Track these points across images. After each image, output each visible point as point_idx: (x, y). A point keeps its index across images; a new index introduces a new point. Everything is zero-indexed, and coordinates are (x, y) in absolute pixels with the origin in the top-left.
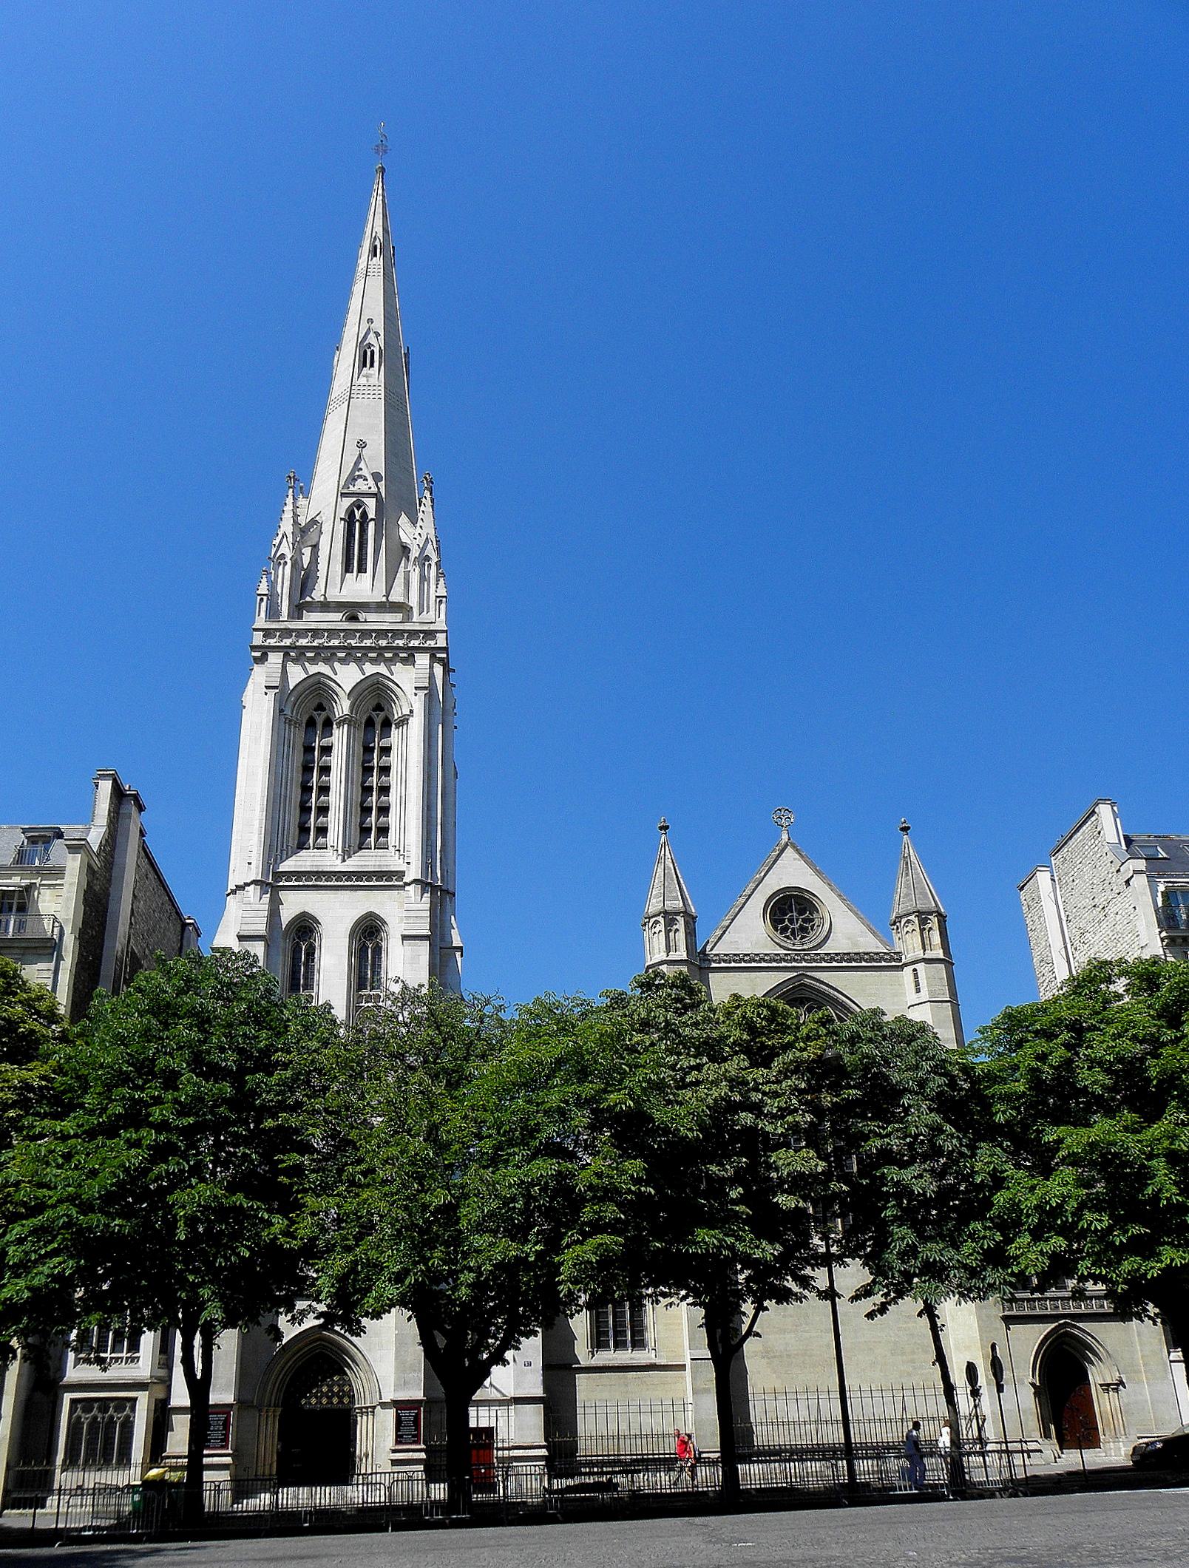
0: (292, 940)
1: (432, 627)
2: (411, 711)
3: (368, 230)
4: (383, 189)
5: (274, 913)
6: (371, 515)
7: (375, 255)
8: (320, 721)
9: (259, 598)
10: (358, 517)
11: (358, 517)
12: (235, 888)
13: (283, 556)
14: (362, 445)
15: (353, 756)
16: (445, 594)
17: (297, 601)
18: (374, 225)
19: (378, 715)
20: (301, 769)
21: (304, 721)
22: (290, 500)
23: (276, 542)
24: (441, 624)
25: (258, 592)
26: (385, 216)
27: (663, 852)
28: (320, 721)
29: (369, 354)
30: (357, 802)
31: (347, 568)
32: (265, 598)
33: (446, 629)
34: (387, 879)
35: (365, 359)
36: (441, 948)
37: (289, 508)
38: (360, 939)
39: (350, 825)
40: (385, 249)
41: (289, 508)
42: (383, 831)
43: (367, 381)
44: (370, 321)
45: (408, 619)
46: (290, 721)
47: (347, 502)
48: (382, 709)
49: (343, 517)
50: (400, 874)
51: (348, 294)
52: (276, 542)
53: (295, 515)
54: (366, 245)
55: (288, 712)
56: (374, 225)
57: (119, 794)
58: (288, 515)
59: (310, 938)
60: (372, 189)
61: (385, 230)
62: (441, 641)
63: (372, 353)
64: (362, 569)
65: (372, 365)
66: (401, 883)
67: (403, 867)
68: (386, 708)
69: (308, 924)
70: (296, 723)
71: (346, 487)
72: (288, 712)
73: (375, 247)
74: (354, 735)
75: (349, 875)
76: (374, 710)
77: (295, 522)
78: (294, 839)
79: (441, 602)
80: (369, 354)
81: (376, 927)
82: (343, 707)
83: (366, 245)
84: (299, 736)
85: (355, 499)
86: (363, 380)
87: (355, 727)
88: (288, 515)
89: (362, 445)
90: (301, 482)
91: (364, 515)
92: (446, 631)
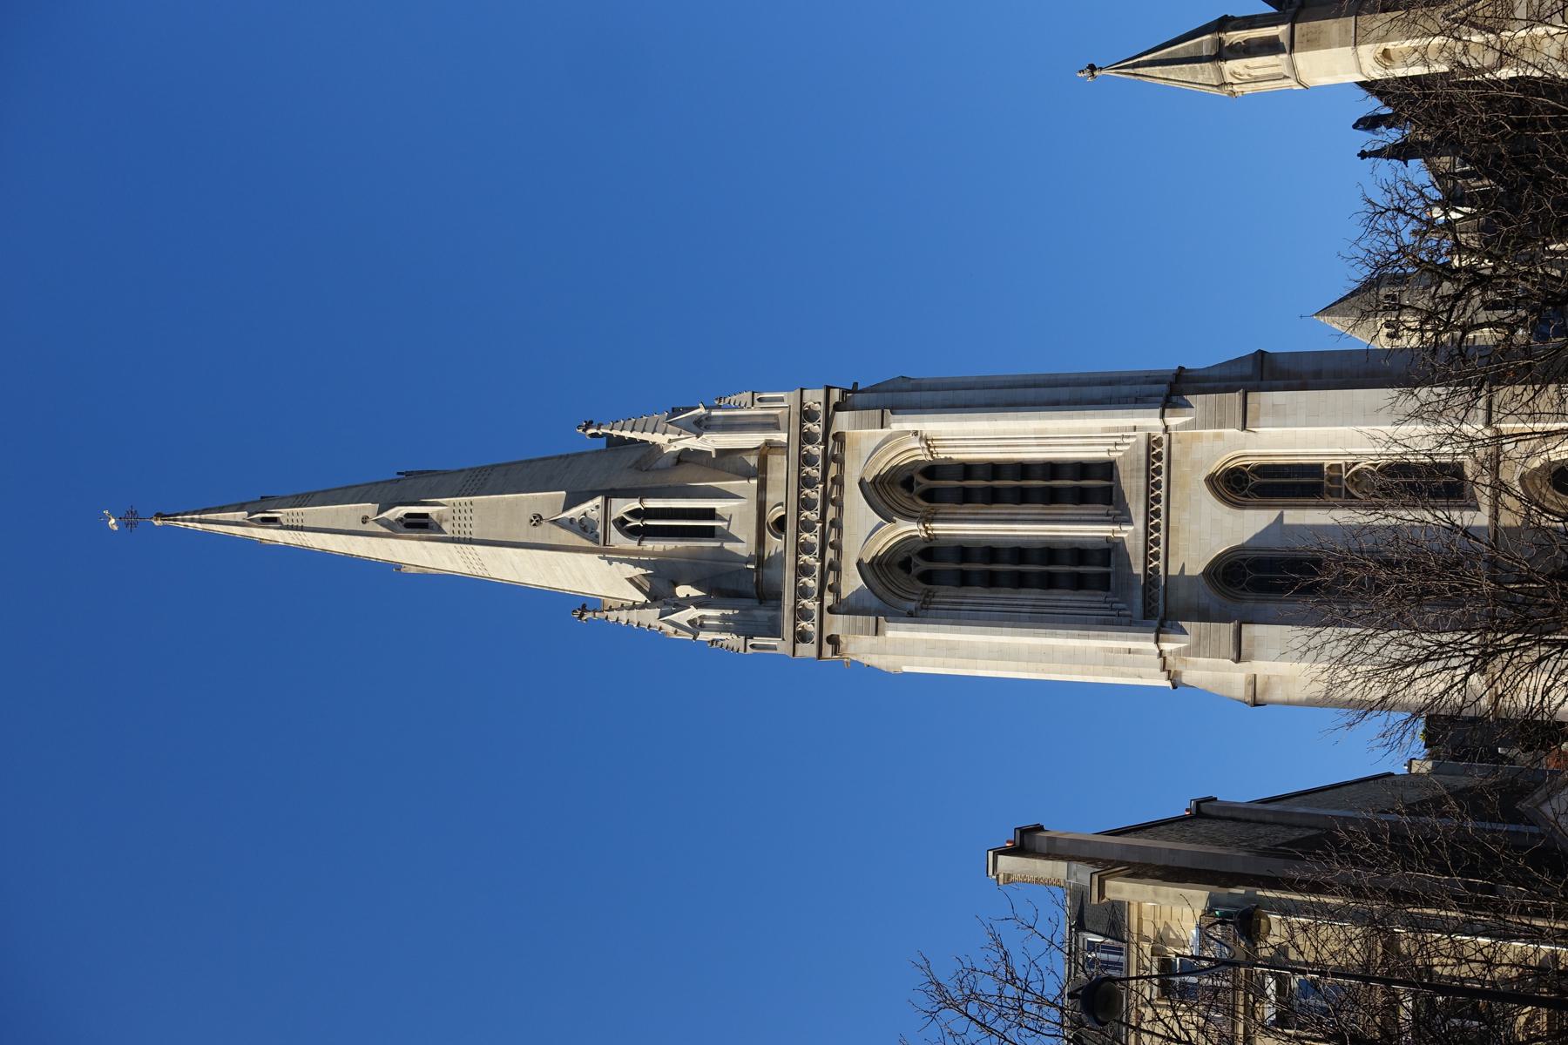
0: (1243, 593)
1: (796, 409)
2: (916, 433)
3: (238, 531)
4: (186, 514)
5: (1203, 615)
6: (635, 504)
7: (275, 520)
8: (924, 566)
9: (750, 651)
10: (638, 523)
11: (638, 523)
12: (1165, 673)
13: (692, 622)
14: (537, 520)
15: (977, 514)
16: (750, 393)
17: (755, 602)
18: (233, 526)
19: (919, 484)
20: (994, 589)
21: (925, 586)
22: (613, 616)
23: (670, 629)
24: (790, 398)
25: (742, 651)
26: (221, 510)
27: (1131, 71)
28: (924, 566)
29: (409, 520)
30: (1043, 509)
31: (709, 533)
32: (750, 642)
33: (799, 390)
34: (1155, 454)
35: (418, 526)
36: (1262, 379)
37: (623, 616)
38: (1246, 496)
39: (1078, 514)
40: (261, 506)
41: (623, 616)
42: (1082, 469)
43: (446, 520)
44: (365, 520)
45: (783, 448)
46: (924, 602)
47: (618, 539)
48: (911, 479)
49: (637, 542)
50: (1152, 443)
51: (326, 556)
52: (670, 629)
53: (634, 606)
54: (259, 533)
55: (912, 606)
56: (233, 526)
57: (1025, 843)
58: (635, 616)
59: (1241, 566)
60: (186, 529)
61: (240, 508)
62: (815, 398)
63: (408, 516)
64: (710, 514)
65: (426, 516)
66: (1165, 437)
67: (1142, 435)
68: (908, 474)
69: (1221, 570)
70: (927, 596)
71: (595, 539)
72: (912, 606)
73: (265, 520)
74: (946, 513)
75: (1151, 514)
76: (911, 489)
77: (644, 606)
78: (1096, 595)
79: (760, 400)
80: (409, 520)
81: (1227, 475)
82: (909, 528)
83: (259, 533)
84: (945, 593)
85: (613, 527)
86: (446, 527)
87: (935, 514)
88: (635, 616)
89: (537, 520)
90: (585, 604)
91: (635, 514)
92: (802, 390)
